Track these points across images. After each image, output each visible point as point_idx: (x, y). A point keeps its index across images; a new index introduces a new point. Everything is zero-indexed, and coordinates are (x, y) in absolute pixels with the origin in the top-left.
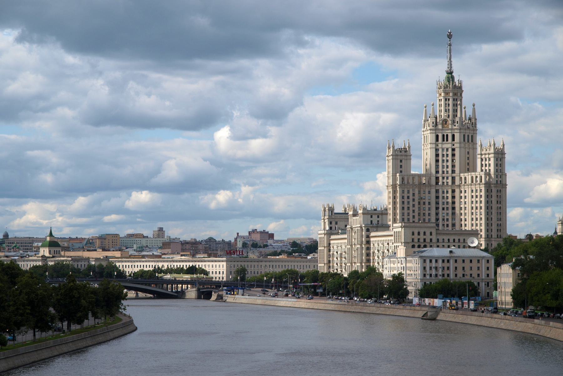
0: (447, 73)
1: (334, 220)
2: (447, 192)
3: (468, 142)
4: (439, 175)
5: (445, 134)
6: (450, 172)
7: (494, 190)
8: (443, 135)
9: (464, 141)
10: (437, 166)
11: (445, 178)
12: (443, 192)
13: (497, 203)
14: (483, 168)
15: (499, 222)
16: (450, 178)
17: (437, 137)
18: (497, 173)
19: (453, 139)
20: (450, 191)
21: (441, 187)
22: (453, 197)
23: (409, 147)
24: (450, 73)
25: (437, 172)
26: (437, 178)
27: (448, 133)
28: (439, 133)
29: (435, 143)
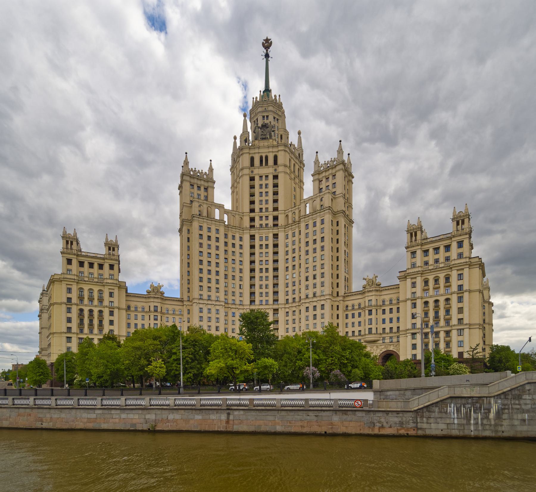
2: (267, 239)
4: (256, 214)
6: (271, 209)
8: (261, 158)
10: (252, 203)
11: (264, 218)
12: (261, 239)
16: (271, 218)
17: (252, 159)
19: (276, 162)
20: (271, 236)
22: (276, 246)
23: (211, 169)
25: (252, 211)
27: (269, 152)
28: (255, 153)
29: (249, 169)
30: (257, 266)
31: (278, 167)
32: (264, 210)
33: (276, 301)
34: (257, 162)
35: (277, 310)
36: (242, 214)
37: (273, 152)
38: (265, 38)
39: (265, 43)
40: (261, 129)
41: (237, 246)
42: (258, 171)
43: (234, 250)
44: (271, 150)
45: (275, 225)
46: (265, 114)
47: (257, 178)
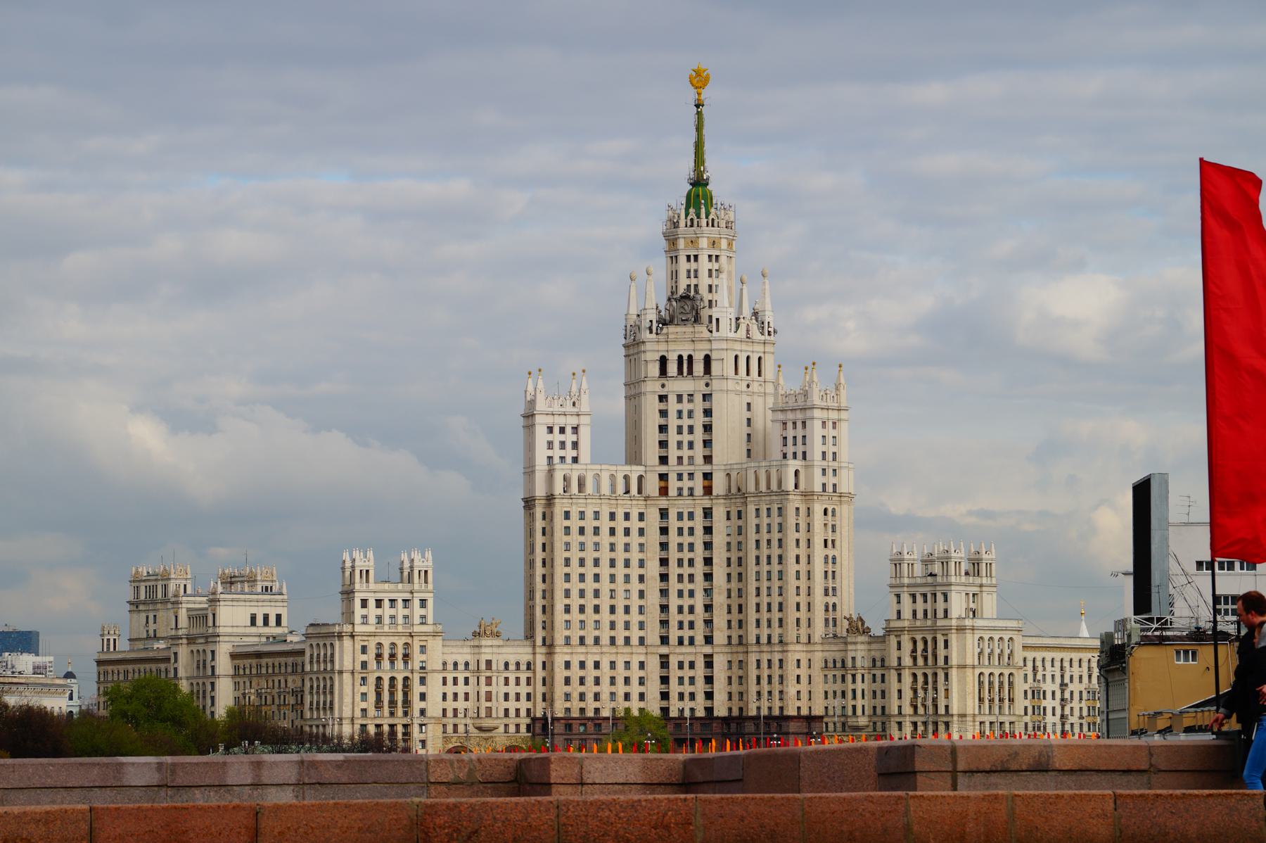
0: (691, 184)
1: (372, 594)
2: (691, 516)
3: (748, 374)
4: (671, 468)
5: (685, 358)
6: (699, 460)
7: (818, 509)
9: (736, 373)
10: (663, 444)
11: (685, 477)
12: (680, 516)
13: (826, 546)
14: (790, 449)
15: (831, 600)
17: (663, 361)
18: (825, 463)
20: (699, 514)
21: (671, 502)
24: (699, 182)
25: (664, 460)
26: (663, 477)
30: (674, 570)
31: (711, 379)
32: (685, 461)
33: (709, 640)
34: (672, 368)
35: (711, 656)
36: (642, 468)
37: (702, 350)
38: (696, 68)
39: (696, 77)
40: (679, 301)
41: (634, 532)
42: (677, 386)
43: (627, 540)
44: (700, 346)
45: (708, 490)
46: (692, 253)
47: (672, 399)
